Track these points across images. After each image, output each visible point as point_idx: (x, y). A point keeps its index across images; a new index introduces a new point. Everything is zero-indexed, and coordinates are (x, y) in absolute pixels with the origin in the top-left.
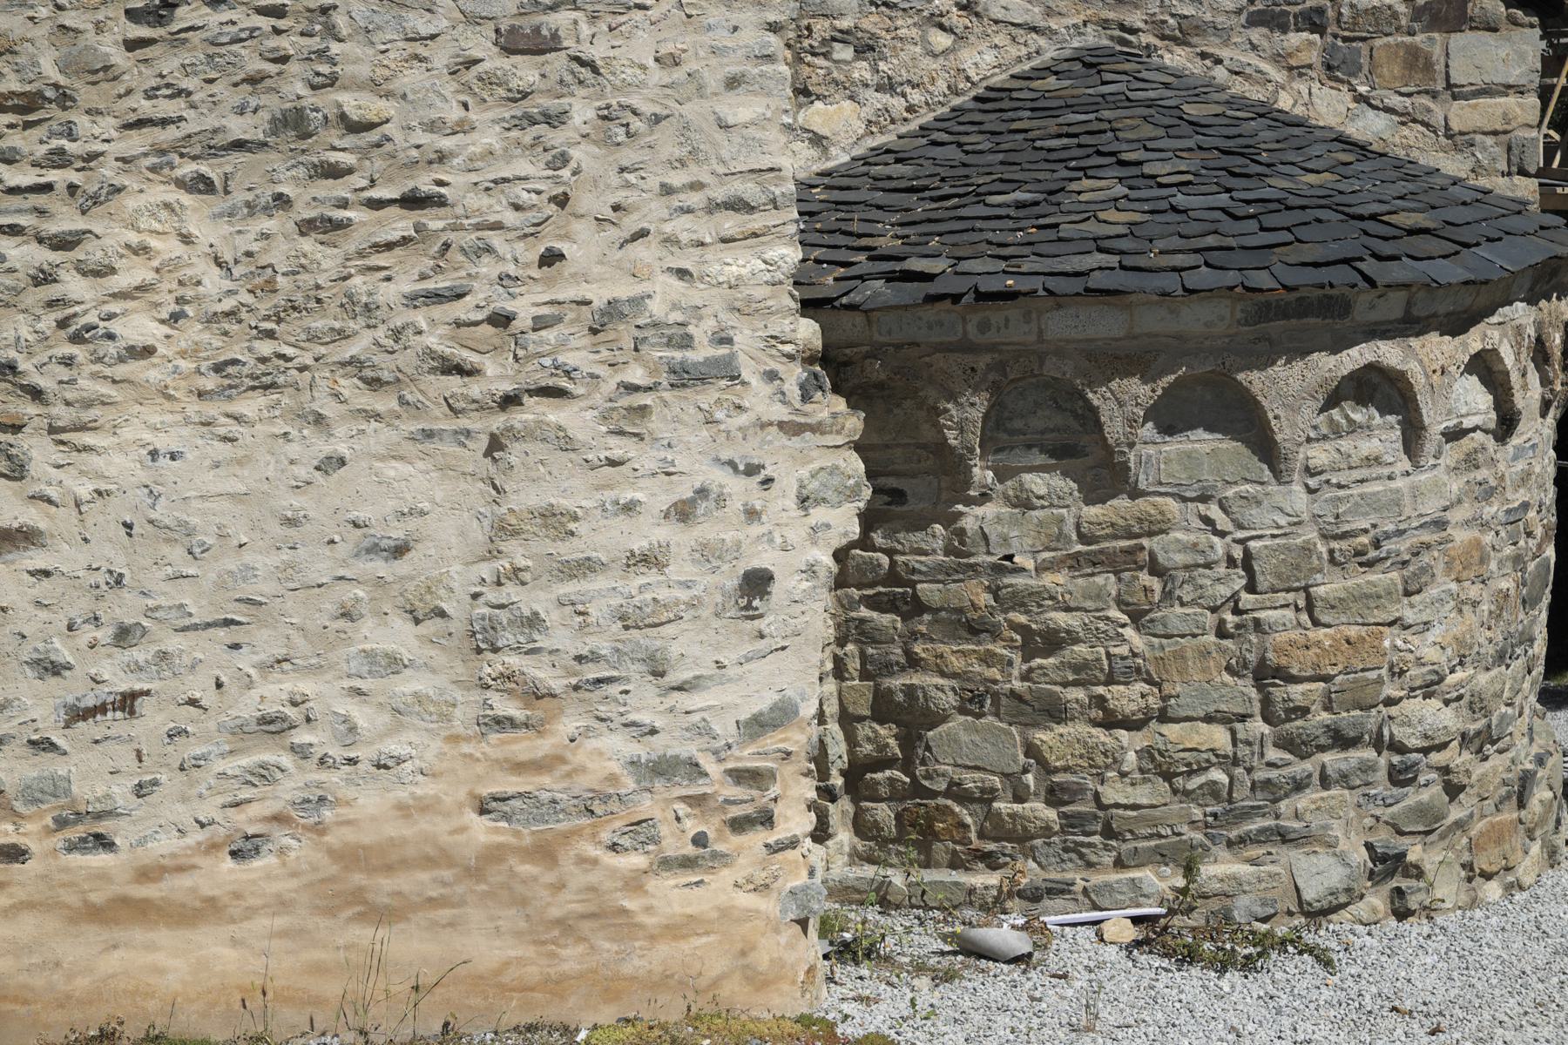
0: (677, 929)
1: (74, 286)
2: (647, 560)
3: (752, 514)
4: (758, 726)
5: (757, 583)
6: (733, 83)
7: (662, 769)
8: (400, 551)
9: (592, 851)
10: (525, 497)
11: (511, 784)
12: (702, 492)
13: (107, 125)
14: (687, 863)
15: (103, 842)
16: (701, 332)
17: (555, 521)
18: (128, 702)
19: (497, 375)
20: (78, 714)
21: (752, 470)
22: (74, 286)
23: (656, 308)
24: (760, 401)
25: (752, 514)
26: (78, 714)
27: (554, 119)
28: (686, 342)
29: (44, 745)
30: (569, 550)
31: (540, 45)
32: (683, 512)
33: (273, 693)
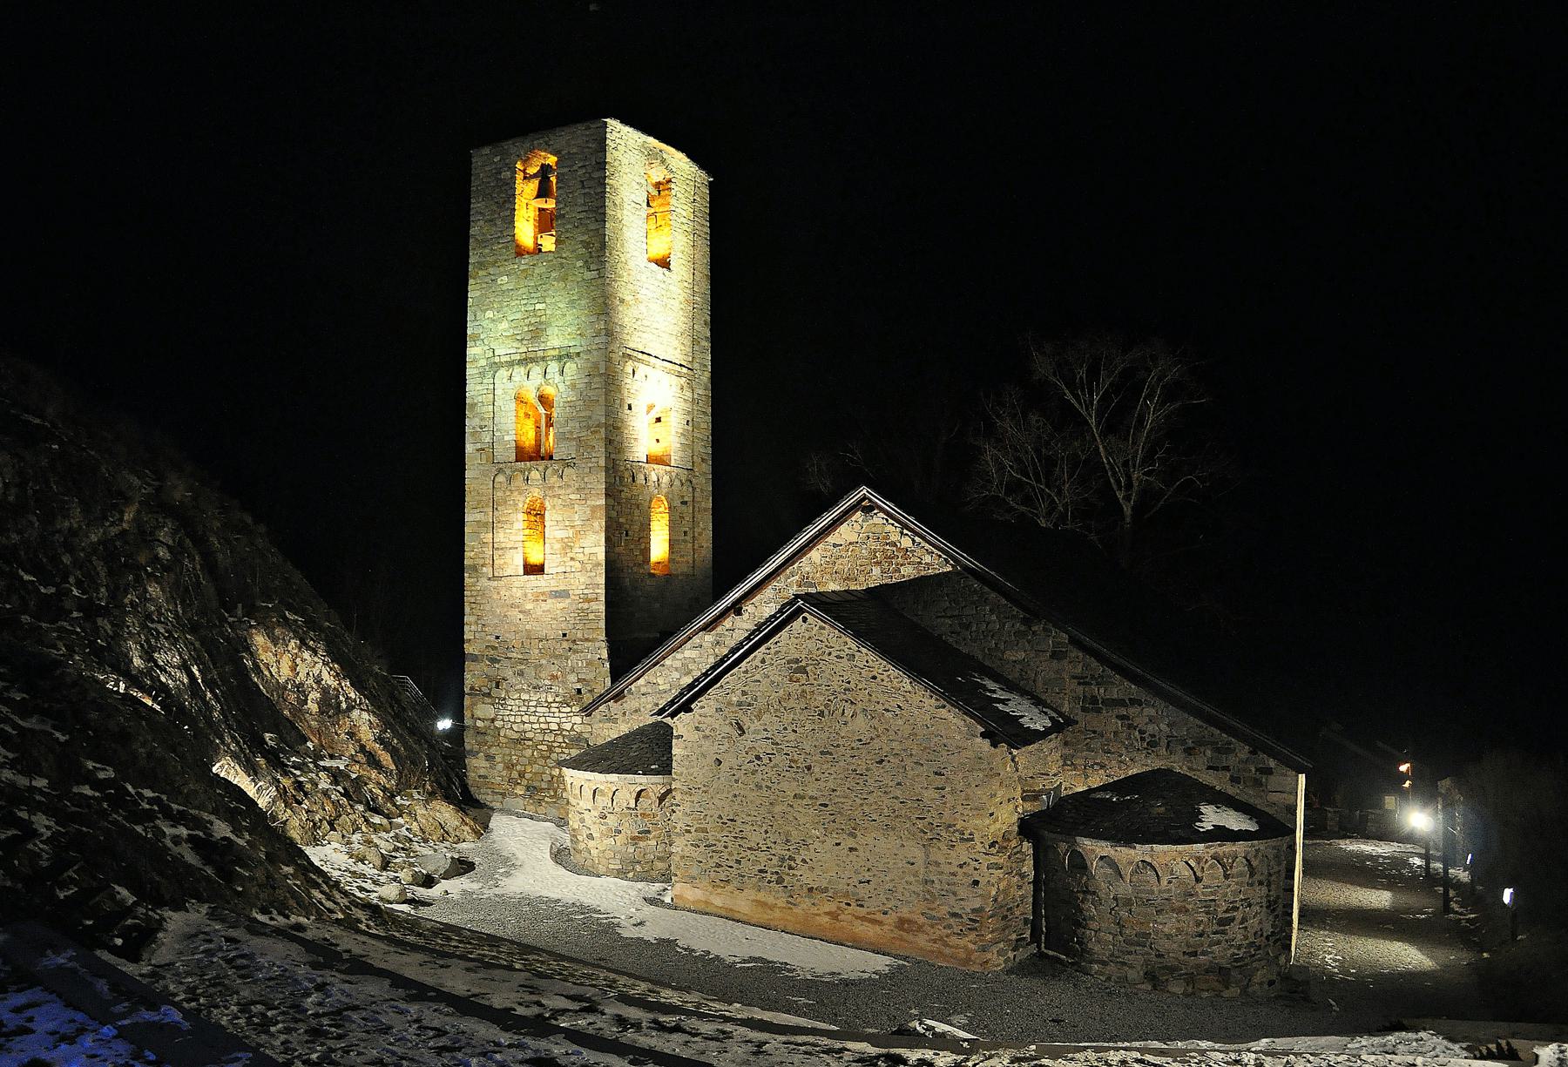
0: (957, 947)
1: (865, 807)
2: (954, 874)
3: (976, 869)
4: (974, 911)
5: (976, 883)
6: (976, 786)
7: (955, 915)
8: (913, 864)
9: (940, 928)
10: (932, 858)
11: (927, 911)
12: (965, 863)
13: (872, 781)
14: (958, 934)
15: (862, 906)
16: (967, 833)
17: (937, 864)
18: (868, 882)
19: (929, 835)
20: (861, 882)
21: (976, 861)
22: (865, 807)
23: (958, 827)
24: (979, 847)
25: (976, 869)
26: (861, 882)
27: (943, 789)
28: (964, 834)
29: (855, 886)
30: (939, 869)
31: (941, 774)
32: (961, 866)
33: (890, 886)
